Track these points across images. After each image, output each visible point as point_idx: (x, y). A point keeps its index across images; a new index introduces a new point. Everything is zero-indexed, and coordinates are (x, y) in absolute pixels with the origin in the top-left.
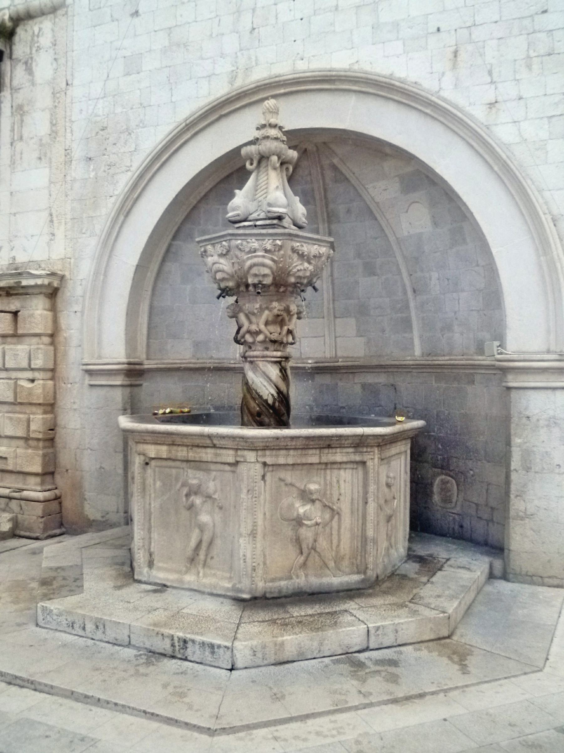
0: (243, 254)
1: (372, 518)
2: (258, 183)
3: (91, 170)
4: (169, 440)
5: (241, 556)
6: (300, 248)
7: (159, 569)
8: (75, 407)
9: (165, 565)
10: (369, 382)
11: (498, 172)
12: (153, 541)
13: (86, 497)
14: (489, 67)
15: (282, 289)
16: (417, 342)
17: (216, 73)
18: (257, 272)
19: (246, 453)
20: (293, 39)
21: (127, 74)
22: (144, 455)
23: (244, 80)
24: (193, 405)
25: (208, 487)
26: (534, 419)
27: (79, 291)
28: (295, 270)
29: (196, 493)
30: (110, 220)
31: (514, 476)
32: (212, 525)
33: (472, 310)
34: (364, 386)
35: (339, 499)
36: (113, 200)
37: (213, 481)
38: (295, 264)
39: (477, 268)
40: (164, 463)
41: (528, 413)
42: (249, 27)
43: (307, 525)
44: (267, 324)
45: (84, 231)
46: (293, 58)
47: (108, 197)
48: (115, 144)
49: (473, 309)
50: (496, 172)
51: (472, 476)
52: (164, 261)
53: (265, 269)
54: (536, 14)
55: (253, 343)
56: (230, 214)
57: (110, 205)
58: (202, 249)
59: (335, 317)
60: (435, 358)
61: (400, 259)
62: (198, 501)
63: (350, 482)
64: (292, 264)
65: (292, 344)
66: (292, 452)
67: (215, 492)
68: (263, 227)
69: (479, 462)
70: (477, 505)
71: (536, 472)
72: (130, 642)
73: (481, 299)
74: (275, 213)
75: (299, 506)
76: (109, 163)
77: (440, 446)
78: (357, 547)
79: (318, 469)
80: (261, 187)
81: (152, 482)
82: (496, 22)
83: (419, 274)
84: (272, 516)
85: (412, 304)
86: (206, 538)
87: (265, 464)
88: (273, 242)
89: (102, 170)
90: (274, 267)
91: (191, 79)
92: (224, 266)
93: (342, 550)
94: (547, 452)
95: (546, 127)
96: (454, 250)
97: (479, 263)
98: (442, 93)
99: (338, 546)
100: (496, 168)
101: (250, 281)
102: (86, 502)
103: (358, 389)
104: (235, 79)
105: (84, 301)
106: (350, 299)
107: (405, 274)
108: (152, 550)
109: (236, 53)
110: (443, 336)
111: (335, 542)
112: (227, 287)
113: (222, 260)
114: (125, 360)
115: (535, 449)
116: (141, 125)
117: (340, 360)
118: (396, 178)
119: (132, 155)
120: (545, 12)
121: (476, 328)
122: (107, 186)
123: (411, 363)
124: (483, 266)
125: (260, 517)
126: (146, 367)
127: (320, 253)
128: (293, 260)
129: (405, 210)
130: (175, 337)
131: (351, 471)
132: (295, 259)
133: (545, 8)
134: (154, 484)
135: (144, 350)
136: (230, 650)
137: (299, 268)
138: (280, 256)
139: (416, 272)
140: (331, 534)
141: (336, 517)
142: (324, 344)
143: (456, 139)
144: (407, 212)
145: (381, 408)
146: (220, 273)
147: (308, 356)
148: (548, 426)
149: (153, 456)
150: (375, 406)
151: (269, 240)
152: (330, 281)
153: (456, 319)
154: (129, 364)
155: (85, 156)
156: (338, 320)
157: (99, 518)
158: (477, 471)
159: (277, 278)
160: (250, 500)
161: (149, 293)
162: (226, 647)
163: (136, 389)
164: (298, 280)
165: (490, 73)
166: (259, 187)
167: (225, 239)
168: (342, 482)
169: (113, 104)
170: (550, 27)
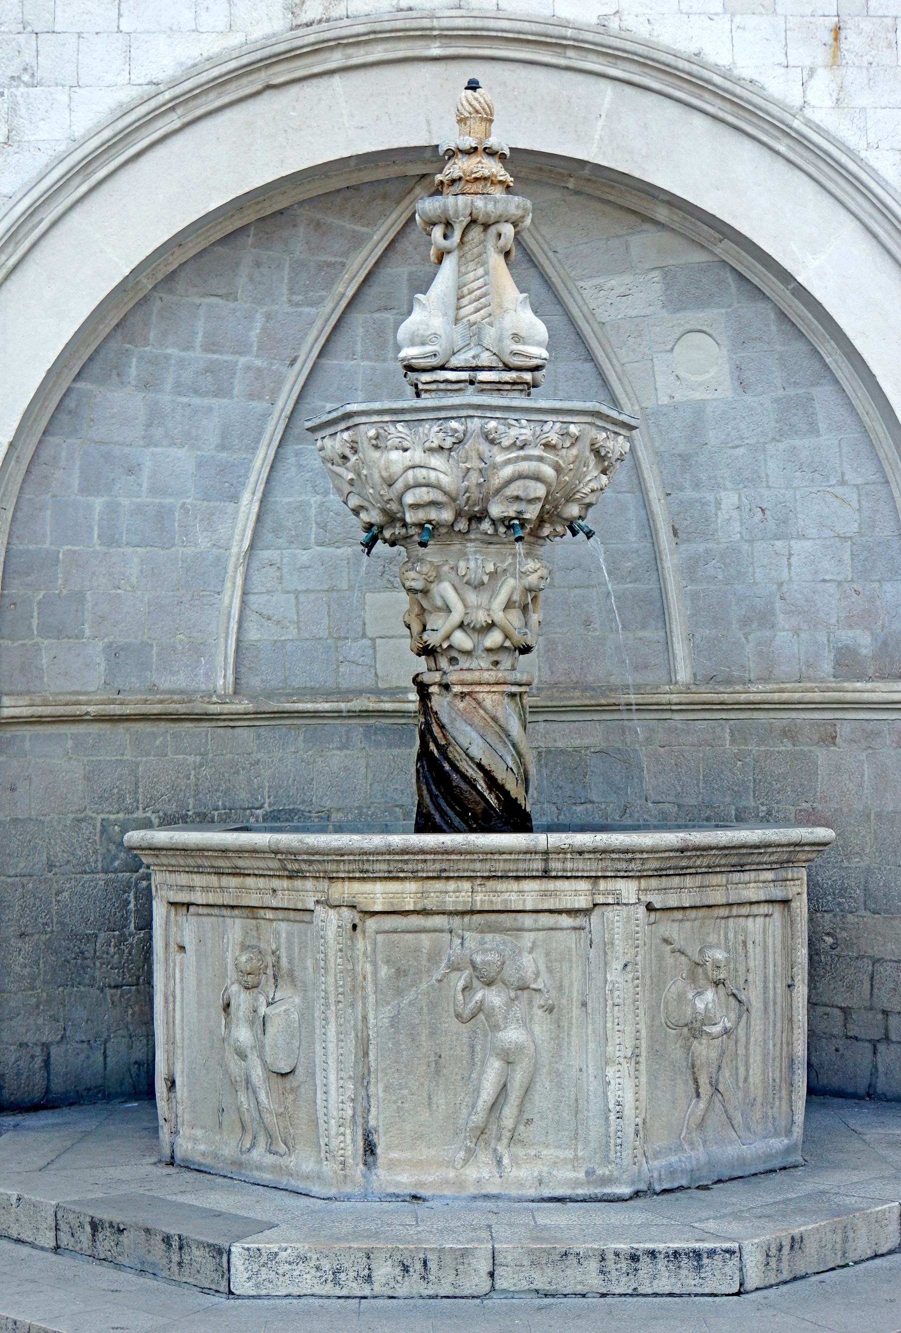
0: (495, 449)
5: (611, 1106)
7: (392, 1165)
9: (408, 1155)
10: (559, 744)
12: (373, 1102)
16: (680, 648)
18: (521, 494)
19: (621, 884)
23: (326, 9)
24: (109, 812)
25: (519, 969)
32: (532, 1049)
33: (824, 581)
38: (588, 478)
39: (839, 490)
43: (708, 1034)
49: (827, 577)
60: (738, 688)
63: (762, 944)
66: (688, 881)
67: (537, 975)
68: (497, 387)
69: (850, 916)
70: (846, 1011)
72: (493, 1286)
73: (847, 557)
74: (531, 358)
78: (774, 1081)
80: (470, 293)
81: (369, 968)
83: (689, 494)
86: (518, 1078)
87: (650, 908)
88: (561, 428)
92: (442, 476)
93: (752, 1089)
96: (781, 446)
97: (846, 478)
98: (808, 112)
99: (746, 1080)
101: (496, 510)
107: (655, 494)
108: (372, 1123)
110: (746, 638)
111: (742, 1070)
113: (436, 461)
116: (26, 78)
118: (656, 273)
121: (833, 621)
123: (674, 698)
124: (857, 486)
129: (669, 347)
130: (59, 633)
131: (762, 919)
134: (375, 973)
136: (738, 1254)
137: (594, 485)
138: (571, 459)
139: (681, 489)
144: (672, 349)
145: (589, 806)
146: (424, 489)
150: (575, 804)
158: (845, 935)
168: (750, 945)
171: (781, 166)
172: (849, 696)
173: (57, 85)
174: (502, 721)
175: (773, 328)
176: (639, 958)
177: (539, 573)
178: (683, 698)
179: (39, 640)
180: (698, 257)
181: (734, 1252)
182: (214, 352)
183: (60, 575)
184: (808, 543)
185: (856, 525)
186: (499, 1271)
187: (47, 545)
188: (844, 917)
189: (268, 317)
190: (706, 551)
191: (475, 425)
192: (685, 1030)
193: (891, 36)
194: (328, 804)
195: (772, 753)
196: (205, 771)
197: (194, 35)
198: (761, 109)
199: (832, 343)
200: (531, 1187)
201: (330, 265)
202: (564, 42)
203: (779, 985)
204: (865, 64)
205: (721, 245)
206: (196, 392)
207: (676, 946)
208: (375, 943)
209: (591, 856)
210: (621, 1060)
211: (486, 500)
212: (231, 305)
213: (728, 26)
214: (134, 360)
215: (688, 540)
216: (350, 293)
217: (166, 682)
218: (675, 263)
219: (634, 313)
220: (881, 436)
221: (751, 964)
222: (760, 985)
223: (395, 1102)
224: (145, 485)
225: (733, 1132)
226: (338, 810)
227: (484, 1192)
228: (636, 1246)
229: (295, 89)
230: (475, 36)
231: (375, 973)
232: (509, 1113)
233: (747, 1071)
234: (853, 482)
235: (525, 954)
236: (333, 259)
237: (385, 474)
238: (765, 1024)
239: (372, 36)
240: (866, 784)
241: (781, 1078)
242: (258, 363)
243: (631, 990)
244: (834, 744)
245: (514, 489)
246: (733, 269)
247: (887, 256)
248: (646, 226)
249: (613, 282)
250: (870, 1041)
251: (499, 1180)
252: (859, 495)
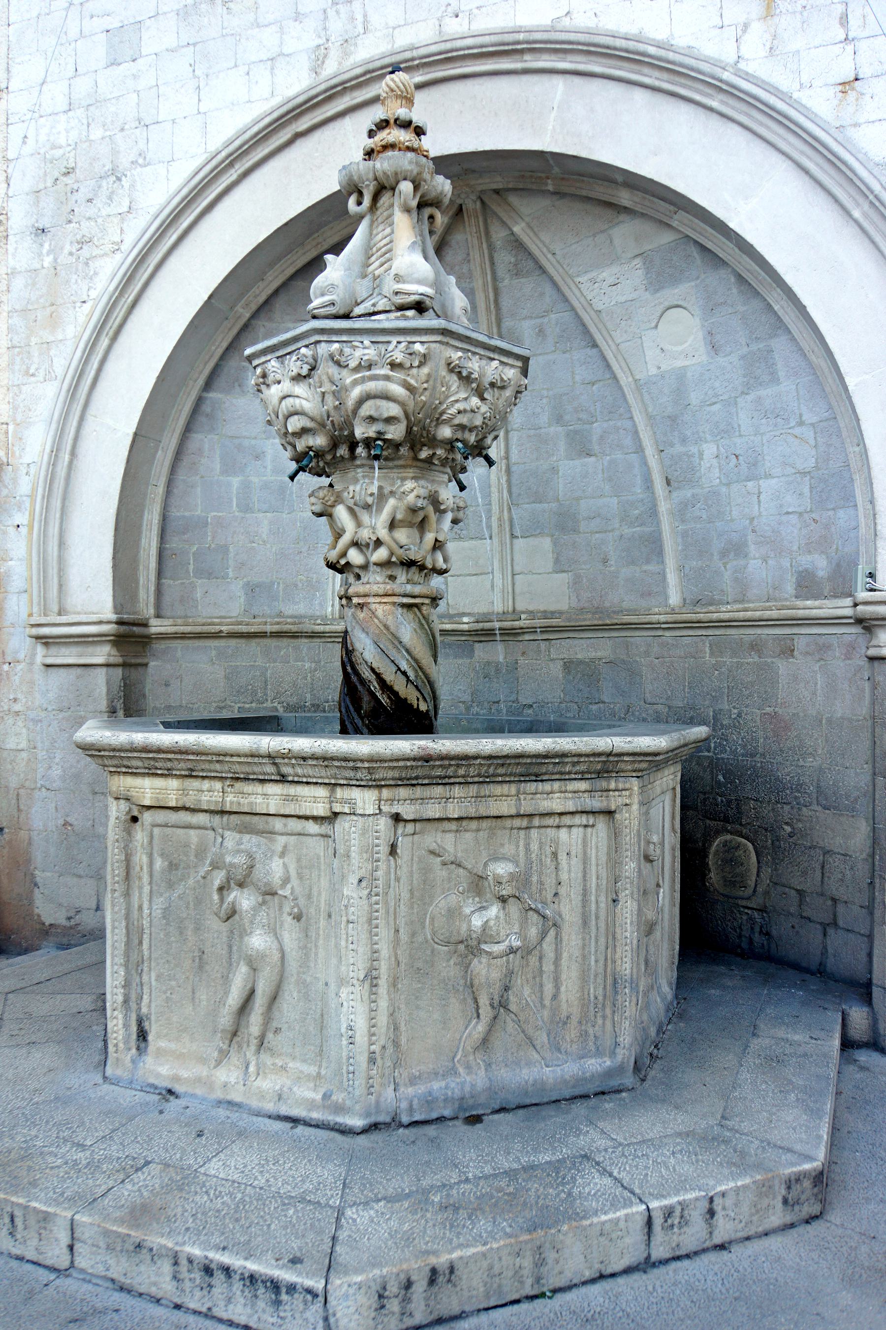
0: (345, 372)
1: (628, 935)
2: (372, 243)
3: (45, 251)
4: (181, 767)
5: (343, 1030)
6: (463, 363)
7: (160, 1053)
8: (17, 707)
9: (173, 1046)
10: (579, 656)
11: (861, 220)
12: (146, 990)
13: (38, 879)
15: (424, 454)
16: (672, 578)
17: (286, 51)
18: (373, 413)
19: (356, 794)
21: (112, 64)
22: (128, 799)
23: (340, 64)
25: (268, 873)
27: (24, 486)
28: (453, 411)
29: (241, 885)
30: (82, 345)
32: (276, 956)
33: (788, 513)
34: (568, 665)
35: (556, 894)
36: (87, 307)
37: (282, 855)
38: (452, 399)
39: (798, 431)
40: (173, 817)
44: (393, 525)
45: (32, 371)
46: (440, 14)
47: (79, 304)
48: (90, 201)
49: (790, 510)
50: (856, 221)
51: (791, 835)
52: (188, 429)
53: (391, 405)
55: (365, 567)
56: (316, 303)
57: (82, 319)
58: (259, 371)
59: (513, 536)
60: (711, 608)
61: (639, 418)
62: (245, 900)
63: (580, 856)
64: (447, 397)
65: (442, 572)
66: (457, 791)
67: (286, 880)
69: (804, 809)
72: (72, 1262)
73: (806, 491)
74: (409, 294)
75: (473, 912)
76: (79, 237)
77: (721, 778)
78: (596, 998)
79: (512, 829)
81: (145, 859)
83: (679, 449)
84: (413, 935)
85: (663, 507)
88: (407, 348)
89: (66, 251)
90: (411, 405)
91: (236, 66)
92: (304, 402)
93: (564, 1006)
96: (749, 398)
97: (804, 418)
98: (742, 65)
99: (555, 997)
100: (857, 214)
101: (360, 431)
102: (36, 890)
103: (557, 670)
104: (323, 62)
105: (33, 503)
106: (540, 502)
107: (650, 451)
108: (144, 1010)
109: (325, 11)
111: (549, 988)
112: (310, 448)
113: (300, 389)
114: (113, 617)
117: (523, 616)
118: (638, 261)
119: (123, 220)
121: (795, 548)
123: (662, 618)
124: (812, 425)
125: (384, 934)
126: (153, 630)
127: (502, 379)
128: (448, 388)
129: (653, 325)
130: (210, 575)
131: (581, 829)
132: (454, 388)
134: (151, 864)
135: (152, 599)
136: (321, 1299)
137: (460, 406)
138: (424, 378)
139: (672, 445)
140: (541, 972)
141: (552, 933)
142: (492, 586)
143: (775, 158)
144: (656, 326)
146: (296, 417)
147: (461, 611)
149: (147, 802)
151: (399, 342)
152: (504, 468)
153: (754, 531)
154: (120, 623)
155: (33, 226)
156: (519, 543)
157: (64, 922)
159: (415, 429)
160: (365, 902)
161: (161, 490)
162: (309, 1291)
163: (134, 674)
164: (459, 435)
166: (374, 249)
167: (306, 342)
168: (562, 857)
169: (85, 122)
171: (715, 122)
172: (801, 613)
174: (392, 628)
175: (735, 291)
176: (379, 873)
177: (415, 493)
178: (669, 618)
179: (194, 580)
180: (667, 237)
181: (316, 1296)
184: (774, 481)
185: (813, 460)
186: (77, 1246)
188: (800, 809)
190: (693, 495)
191: (323, 349)
192: (461, 947)
195: (742, 664)
196: (318, 674)
198: (692, 69)
199: (779, 290)
200: (270, 1101)
202: (519, 47)
203: (602, 898)
204: (799, 8)
205: (676, 217)
207: (447, 858)
208: (151, 837)
209: (314, 762)
210: (355, 982)
211: (348, 424)
215: (679, 488)
217: (290, 609)
218: (650, 247)
219: (623, 299)
221: (564, 876)
222: (577, 899)
223: (165, 992)
224: (269, 467)
225: (534, 1053)
227: (229, 1098)
228: (211, 1255)
230: (449, 59)
231: (151, 864)
232: (255, 1020)
233: (557, 987)
234: (810, 421)
235: (276, 858)
238: (584, 939)
239: (368, 76)
240: (819, 692)
241: (605, 996)
243: (366, 908)
244: (793, 656)
246: (696, 242)
247: (819, 190)
248: (622, 217)
249: (604, 274)
250: (821, 924)
251: (242, 1088)
252: (815, 433)
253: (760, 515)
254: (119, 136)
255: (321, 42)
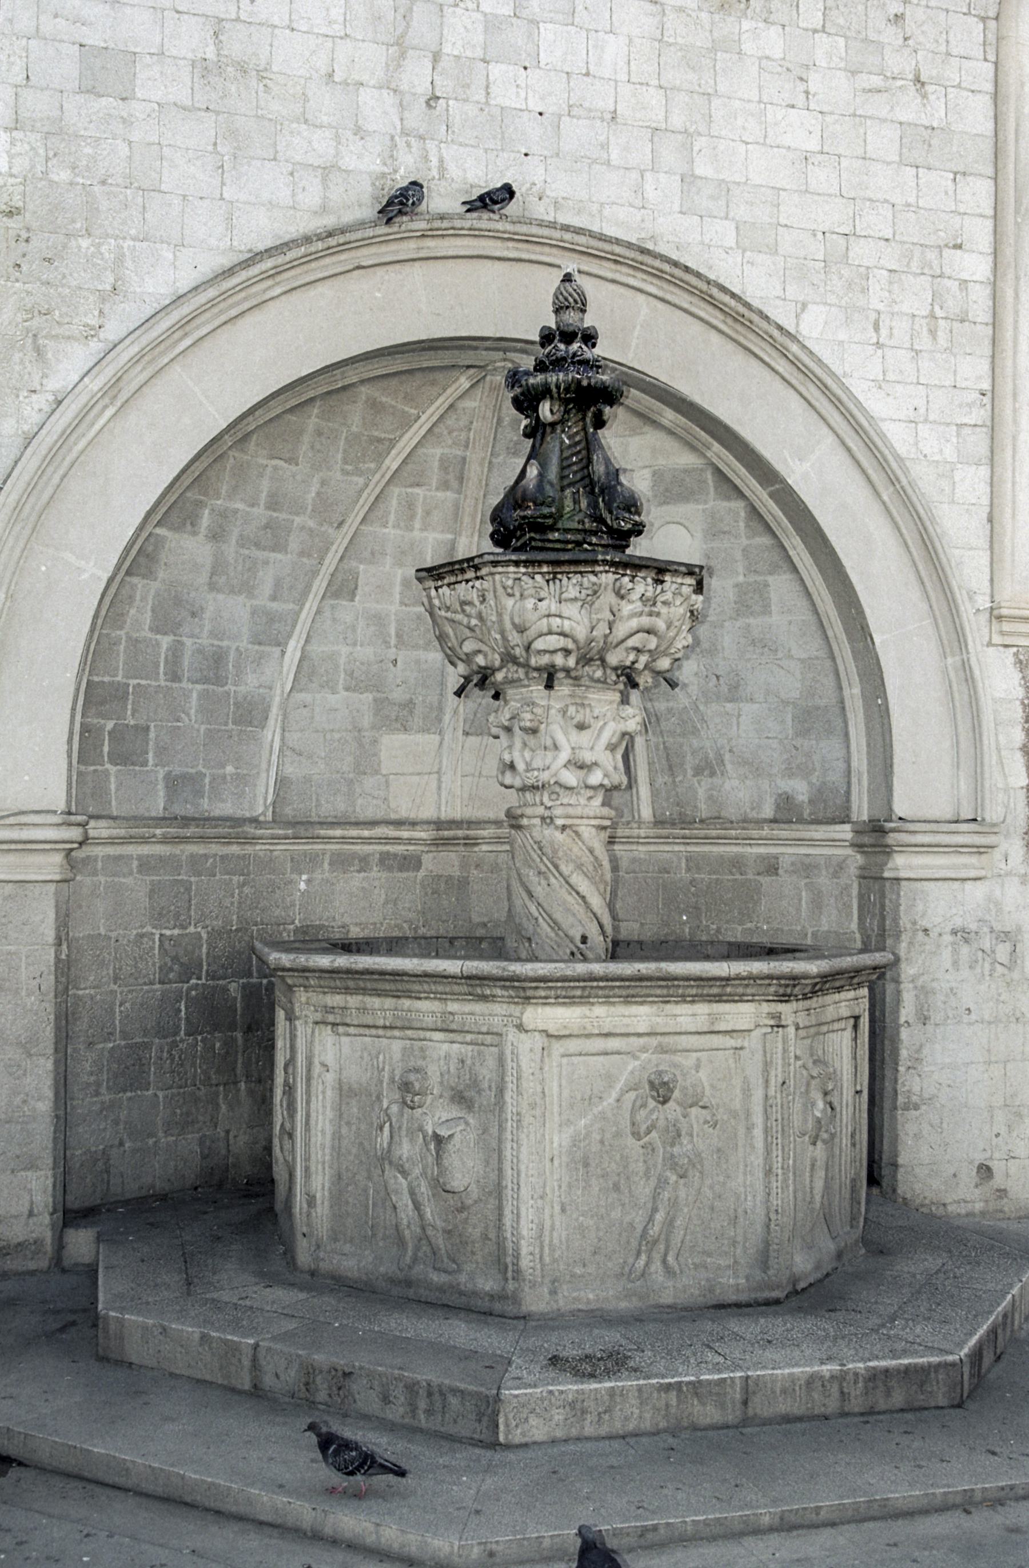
14: (873, 316)
20: (524, 151)
26: (933, 934)
31: (904, 1034)
39: (784, 663)
41: (924, 923)
42: (423, 88)
48: (49, 260)
50: (884, 503)
54: (946, 246)
71: (936, 1025)
82: (887, 240)
91: (275, 159)
92: (574, 625)
94: (951, 989)
95: (954, 440)
96: (738, 624)
113: (571, 610)
115: (935, 985)
119: (103, 300)
120: (959, 247)
122: (22, 362)
124: (802, 661)
133: (959, 241)
148: (953, 943)
165: (877, 327)
170: (965, 276)
173: (162, 242)
175: (742, 524)
179: (108, 766)
180: (687, 459)
182: (275, 510)
183: (129, 707)
184: (757, 706)
187: (119, 678)
189: (323, 483)
193: (864, 283)
194: (347, 920)
196: (246, 890)
197: (292, 212)
201: (379, 440)
206: (257, 545)
208: (560, 1066)
212: (294, 468)
213: (739, 259)
214: (207, 512)
216: (395, 466)
220: (833, 619)
226: (356, 924)
229: (380, 271)
236: (383, 436)
237: (517, 621)
239: (451, 232)
242: (311, 524)
245: (632, 642)
248: (647, 429)
253: (739, 736)
254: (97, 189)
255: (387, 170)
